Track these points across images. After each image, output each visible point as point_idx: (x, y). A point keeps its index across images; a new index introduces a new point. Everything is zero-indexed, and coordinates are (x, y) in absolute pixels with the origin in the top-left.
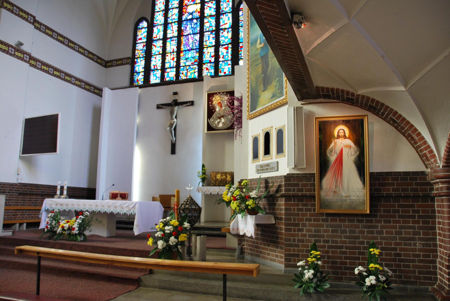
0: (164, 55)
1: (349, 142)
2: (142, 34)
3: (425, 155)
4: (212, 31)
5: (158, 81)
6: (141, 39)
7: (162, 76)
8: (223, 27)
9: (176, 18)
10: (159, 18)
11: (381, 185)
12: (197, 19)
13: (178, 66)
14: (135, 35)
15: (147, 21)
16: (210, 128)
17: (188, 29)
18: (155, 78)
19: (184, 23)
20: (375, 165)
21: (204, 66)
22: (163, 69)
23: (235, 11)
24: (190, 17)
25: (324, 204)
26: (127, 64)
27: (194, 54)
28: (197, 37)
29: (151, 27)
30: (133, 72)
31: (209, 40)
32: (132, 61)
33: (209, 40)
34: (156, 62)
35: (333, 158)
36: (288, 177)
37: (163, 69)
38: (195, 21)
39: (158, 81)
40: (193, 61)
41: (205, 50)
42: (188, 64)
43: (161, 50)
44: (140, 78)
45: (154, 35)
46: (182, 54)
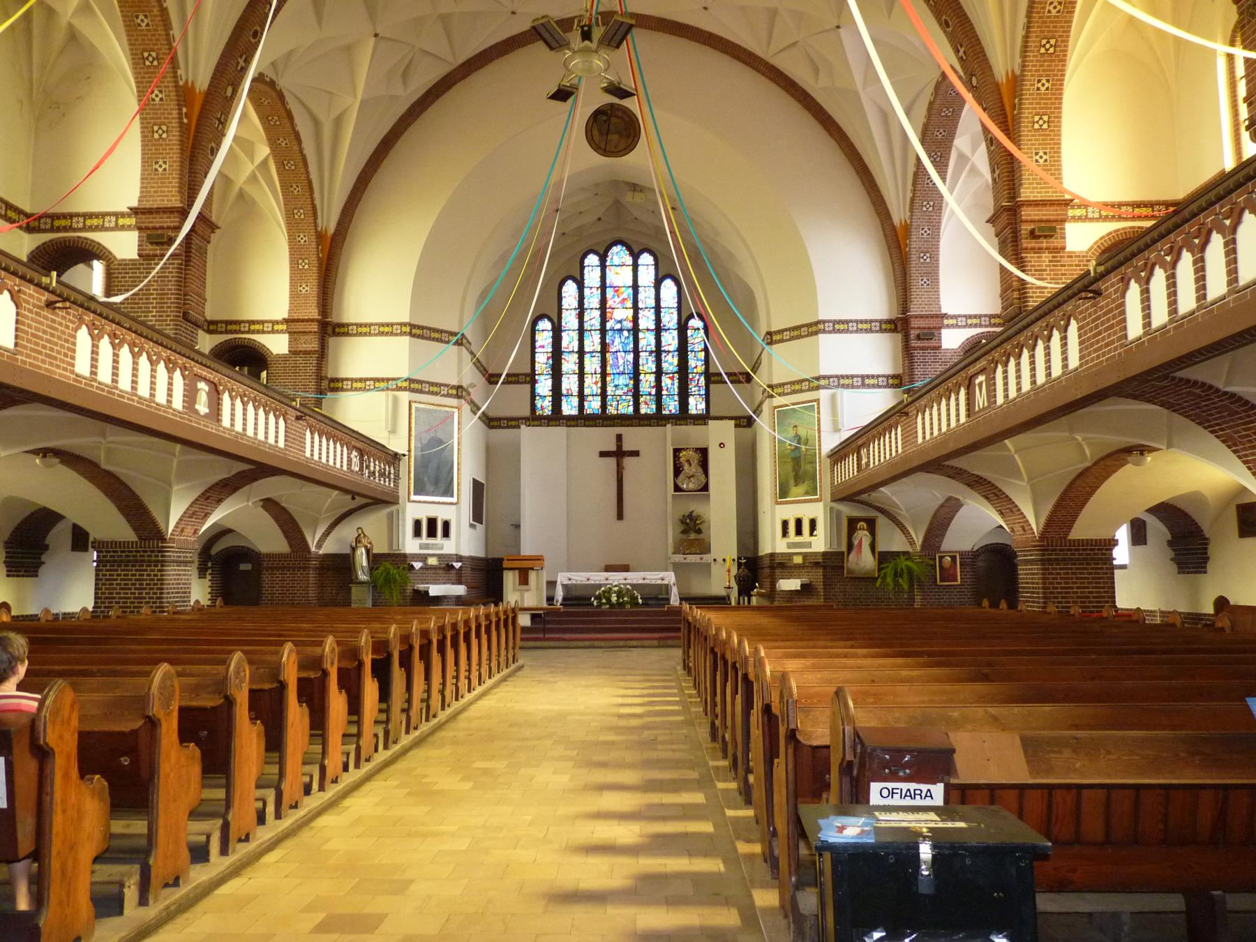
0: (581, 375)
1: (866, 533)
2: (544, 339)
3: (912, 543)
4: (651, 352)
5: (575, 412)
6: (543, 347)
7: (581, 406)
8: (666, 348)
9: (596, 323)
10: (570, 320)
11: (884, 558)
12: (629, 331)
13: (603, 395)
14: (533, 341)
15: (550, 320)
16: (677, 488)
17: (618, 343)
18: (569, 407)
19: (610, 333)
20: (881, 547)
21: (642, 399)
22: (582, 397)
23: (682, 329)
24: (618, 326)
25: (850, 571)
26: (525, 383)
27: (624, 381)
28: (630, 357)
29: (557, 332)
30: (533, 395)
31: (648, 364)
32: (532, 379)
33: (648, 364)
34: (569, 383)
35: (856, 542)
36: (824, 554)
37: (582, 397)
38: (626, 333)
39: (575, 412)
40: (626, 389)
41: (642, 377)
42: (618, 392)
43: (576, 368)
44: (545, 405)
45: (564, 344)
46: (608, 379)
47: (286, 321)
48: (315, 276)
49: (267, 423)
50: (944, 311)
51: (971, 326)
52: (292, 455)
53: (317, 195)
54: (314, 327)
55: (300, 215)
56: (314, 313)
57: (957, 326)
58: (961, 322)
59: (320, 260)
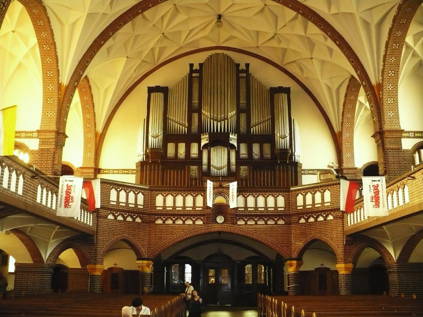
47: (38, 131)
48: (56, 108)
49: (17, 182)
50: (402, 128)
51: (417, 137)
52: (29, 201)
53: (59, 64)
54: (53, 135)
55: (50, 74)
56: (53, 127)
57: (409, 137)
58: (412, 135)
59: (59, 99)
